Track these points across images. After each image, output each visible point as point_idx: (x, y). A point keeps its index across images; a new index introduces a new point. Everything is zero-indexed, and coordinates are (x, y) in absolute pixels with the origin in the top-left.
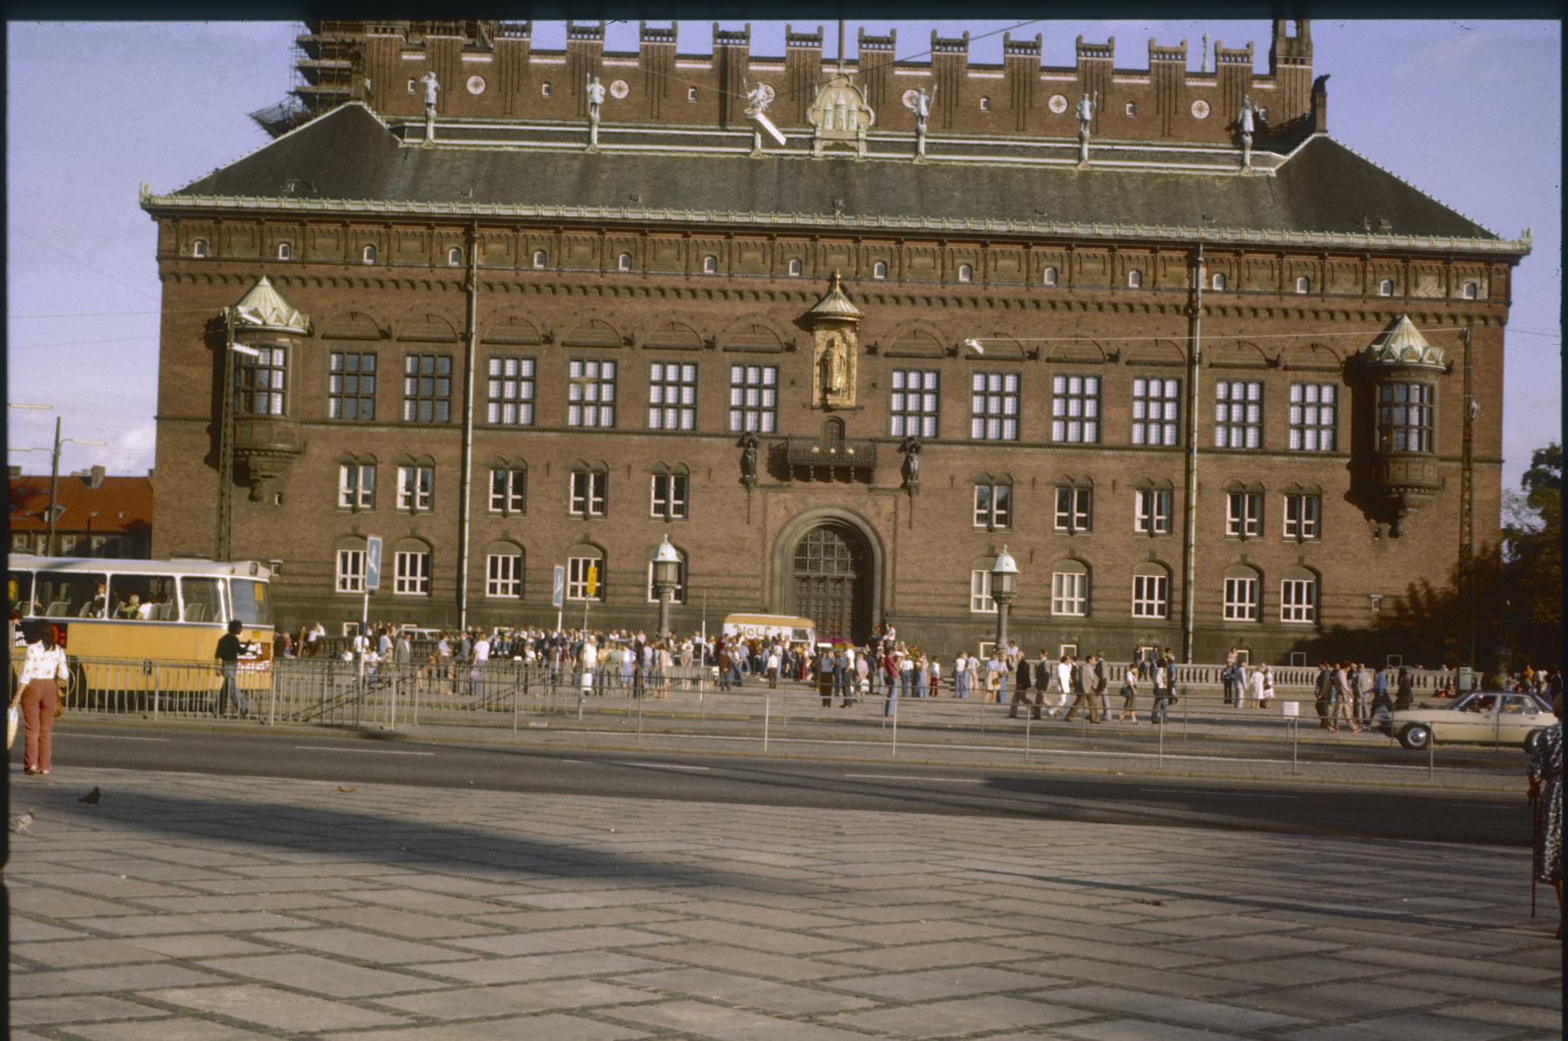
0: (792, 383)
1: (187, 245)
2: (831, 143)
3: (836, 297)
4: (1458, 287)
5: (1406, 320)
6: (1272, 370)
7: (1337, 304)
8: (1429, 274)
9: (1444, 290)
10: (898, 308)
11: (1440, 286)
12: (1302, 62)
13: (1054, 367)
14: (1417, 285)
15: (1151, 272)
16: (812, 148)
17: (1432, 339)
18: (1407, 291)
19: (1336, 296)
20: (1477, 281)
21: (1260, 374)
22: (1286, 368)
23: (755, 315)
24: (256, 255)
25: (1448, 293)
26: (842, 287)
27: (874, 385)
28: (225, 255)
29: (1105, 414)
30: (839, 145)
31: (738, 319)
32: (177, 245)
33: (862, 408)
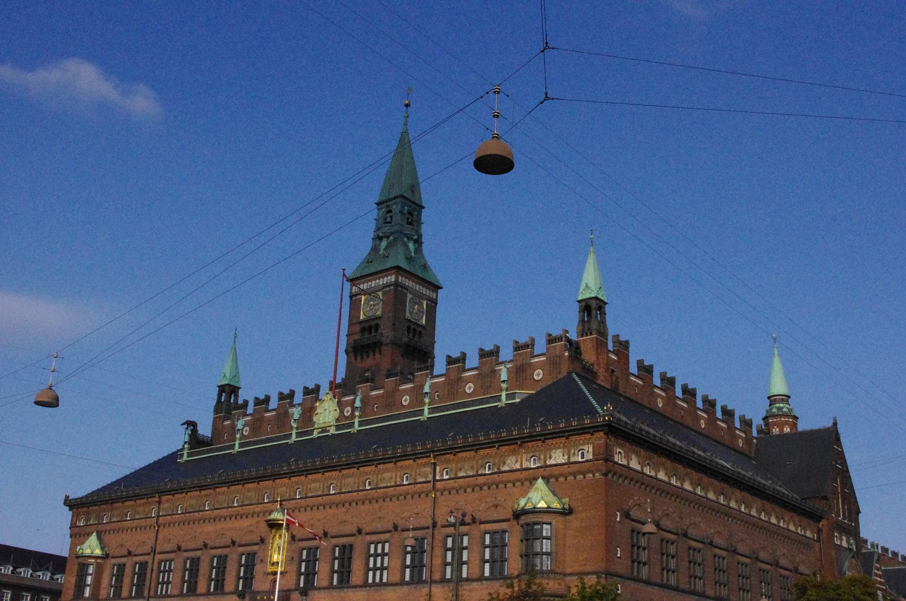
0: (262, 561)
1: (79, 522)
2: (320, 430)
3: (278, 511)
4: (574, 454)
5: (540, 481)
6: (474, 526)
8: (559, 448)
9: (566, 457)
10: (305, 513)
11: (563, 455)
12: (591, 334)
13: (368, 538)
14: (550, 457)
16: (312, 435)
18: (545, 462)
20: (586, 447)
22: (481, 523)
23: (251, 526)
24: (97, 522)
25: (569, 458)
26: (280, 505)
27: (293, 558)
28: (88, 524)
30: (324, 430)
31: (244, 529)
32: (76, 522)
33: (286, 572)
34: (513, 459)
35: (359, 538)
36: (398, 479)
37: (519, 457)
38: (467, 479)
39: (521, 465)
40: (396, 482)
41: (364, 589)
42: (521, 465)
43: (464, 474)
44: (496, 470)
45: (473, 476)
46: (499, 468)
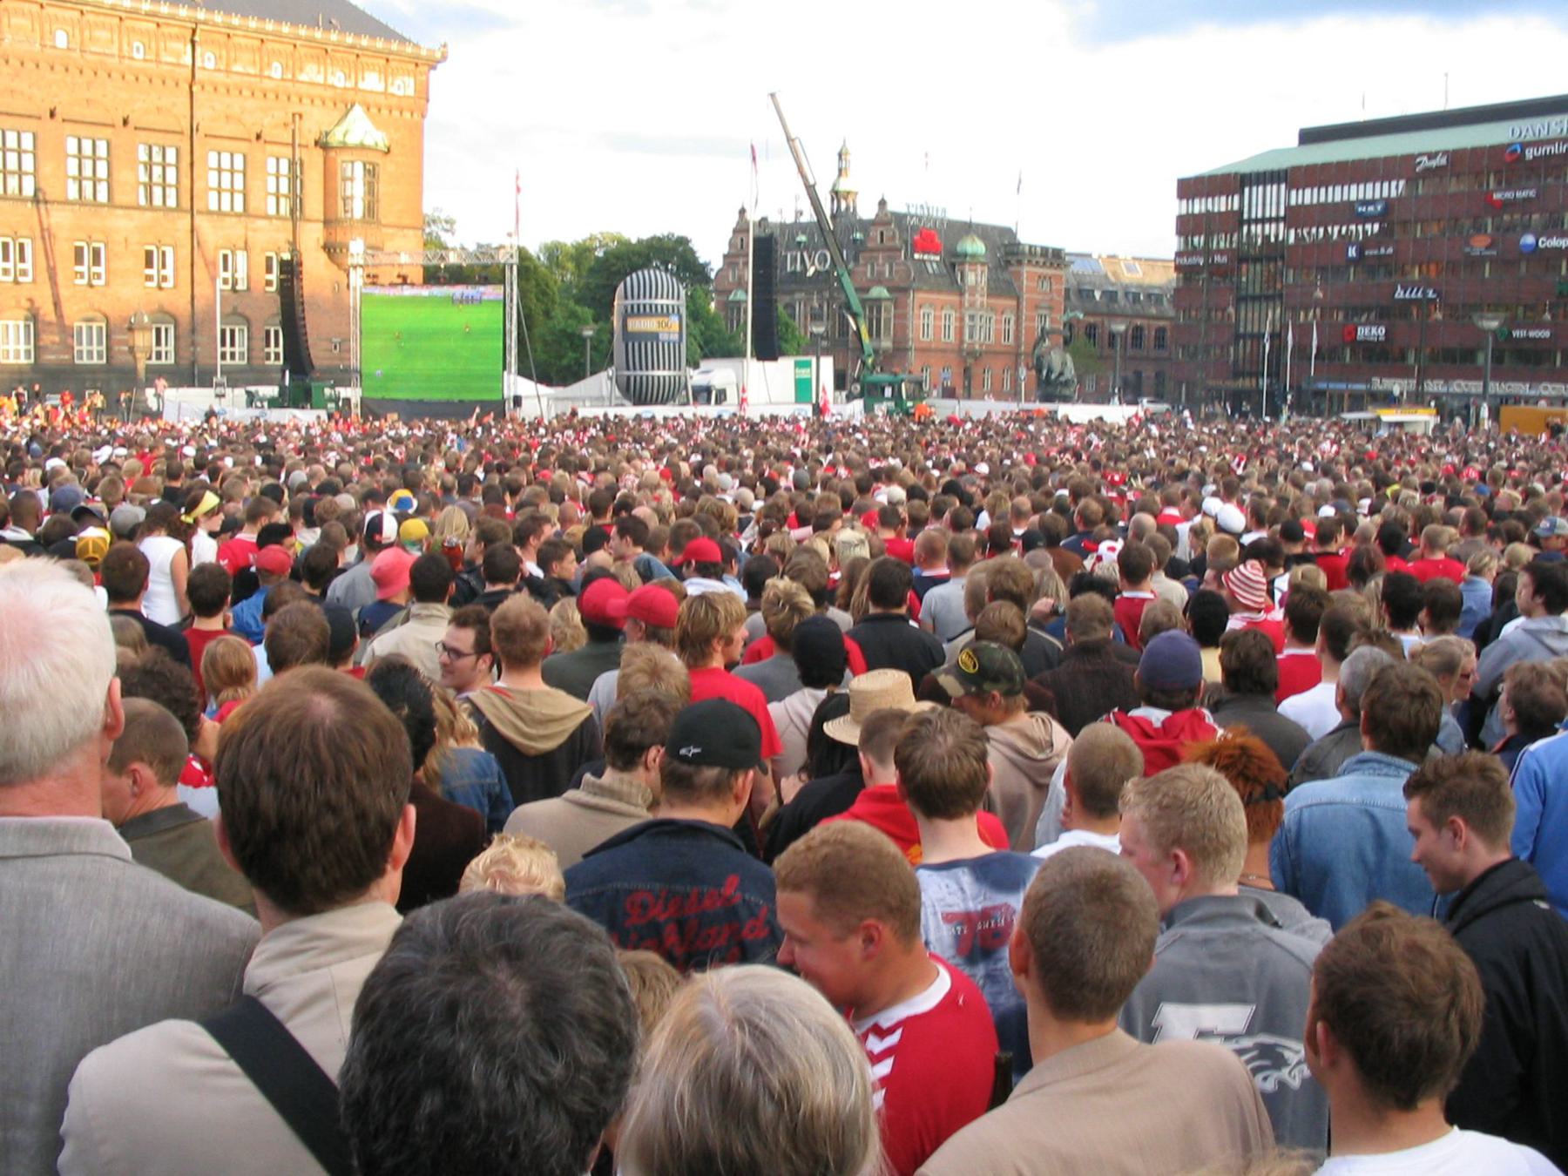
7: (304, 89)
8: (374, 70)
9: (383, 84)
14: (363, 79)
15: (153, 45)
17: (379, 125)
18: (356, 83)
19: (302, 82)
20: (406, 79)
21: (244, 146)
29: (115, 175)
34: (315, 67)
35: (51, 124)
36: (125, 47)
37: (322, 69)
38: (246, 79)
39: (326, 78)
40: (120, 49)
41: (68, 207)
42: (326, 78)
43: (237, 68)
44: (290, 76)
45: (255, 76)
46: (294, 75)
